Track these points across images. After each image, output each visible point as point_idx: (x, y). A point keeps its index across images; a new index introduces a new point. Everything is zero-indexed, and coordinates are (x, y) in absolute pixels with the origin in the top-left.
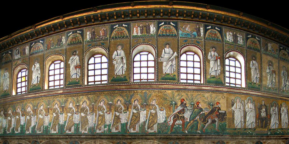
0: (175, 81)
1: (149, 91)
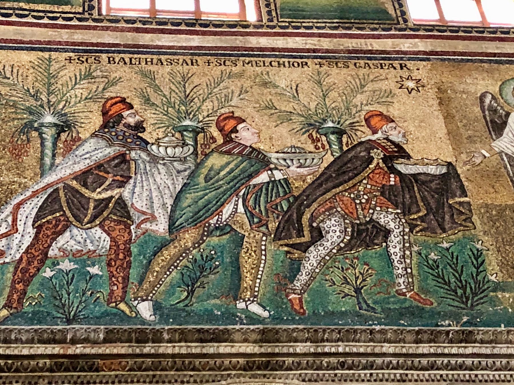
0: (67, 8)
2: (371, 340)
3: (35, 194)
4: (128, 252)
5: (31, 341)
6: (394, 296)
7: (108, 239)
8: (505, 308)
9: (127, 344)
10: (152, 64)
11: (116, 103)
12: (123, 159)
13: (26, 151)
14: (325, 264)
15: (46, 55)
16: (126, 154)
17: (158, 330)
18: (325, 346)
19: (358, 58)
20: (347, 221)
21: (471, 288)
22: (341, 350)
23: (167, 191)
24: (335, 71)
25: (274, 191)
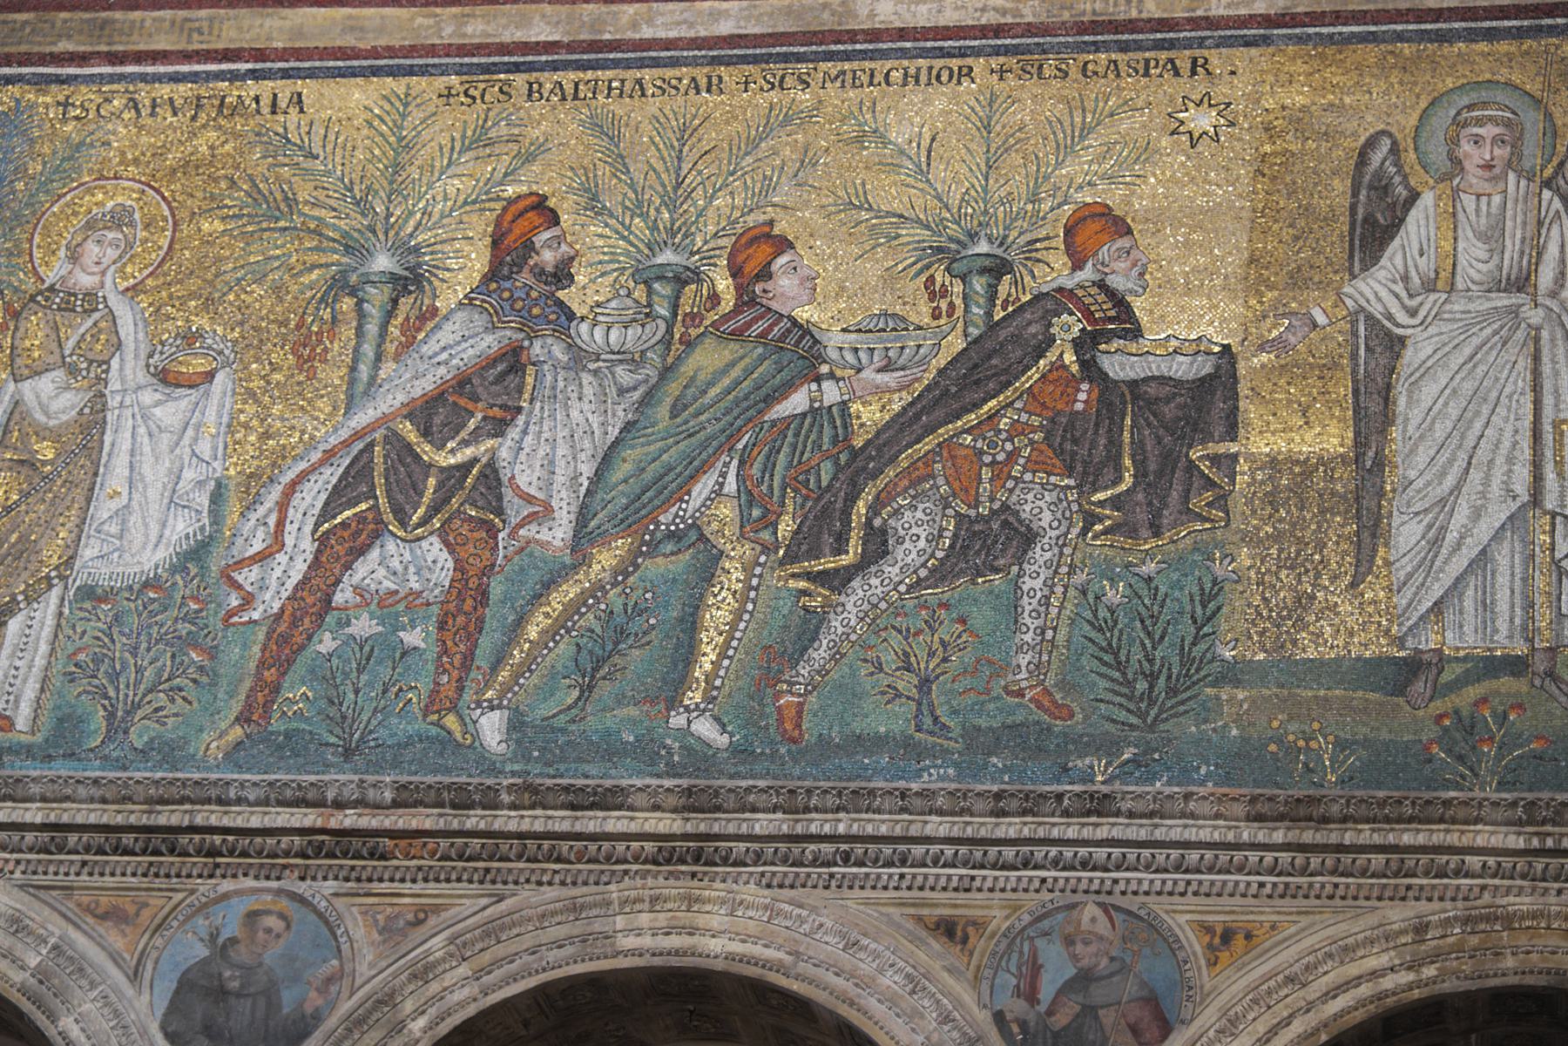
1: (66, 105)
2: (903, 810)
3: (330, 455)
4: (483, 596)
5: (265, 802)
6: (998, 698)
7: (450, 564)
8: (1225, 726)
9: (436, 811)
10: (621, 96)
11: (526, 211)
12: (513, 362)
13: (326, 350)
14: (874, 620)
15: (398, 85)
16: (522, 347)
17: (489, 787)
18: (812, 820)
19: (1097, 47)
20: (950, 512)
21: (1169, 677)
22: (841, 829)
23: (587, 444)
24: (1032, 85)
25: (813, 437)
